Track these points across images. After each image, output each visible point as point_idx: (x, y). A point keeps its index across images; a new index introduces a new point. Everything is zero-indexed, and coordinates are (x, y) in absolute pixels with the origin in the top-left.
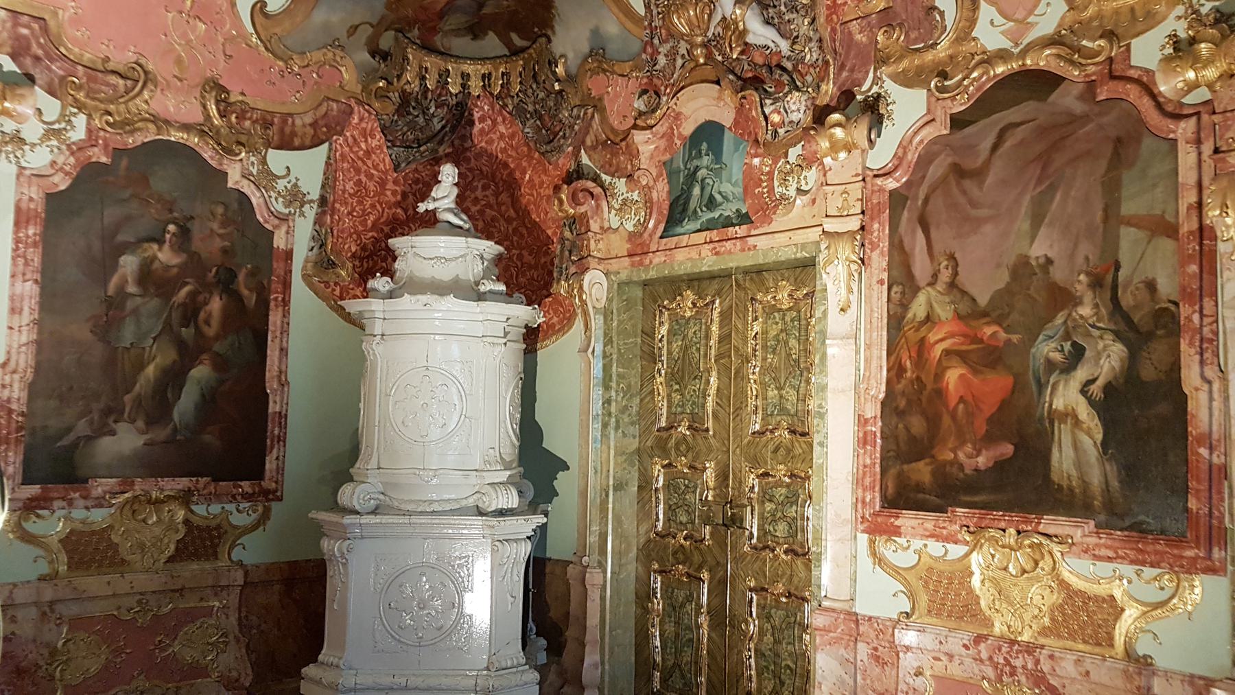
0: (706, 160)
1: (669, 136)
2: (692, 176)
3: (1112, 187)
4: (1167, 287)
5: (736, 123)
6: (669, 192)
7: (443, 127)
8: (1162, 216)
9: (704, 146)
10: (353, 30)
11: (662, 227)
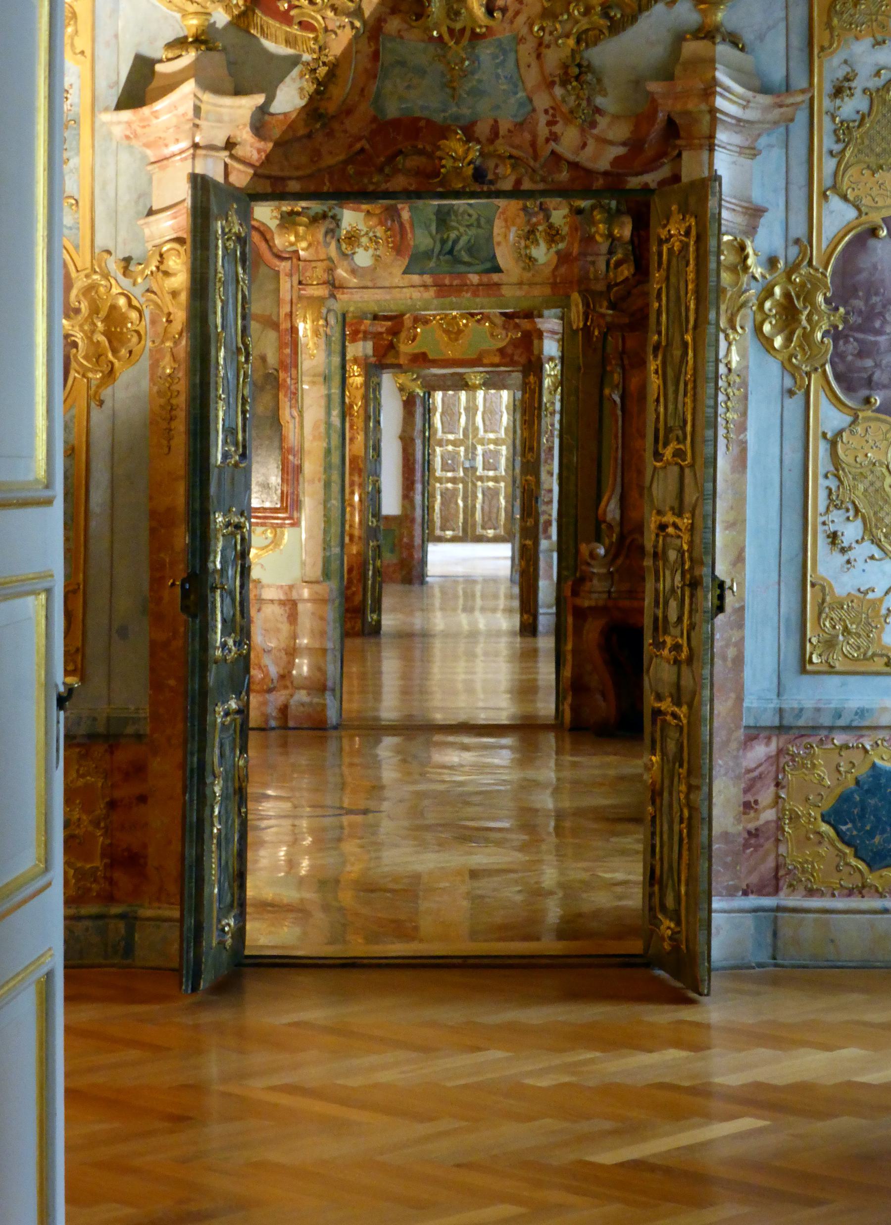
4: (272, 360)
8: (270, 316)
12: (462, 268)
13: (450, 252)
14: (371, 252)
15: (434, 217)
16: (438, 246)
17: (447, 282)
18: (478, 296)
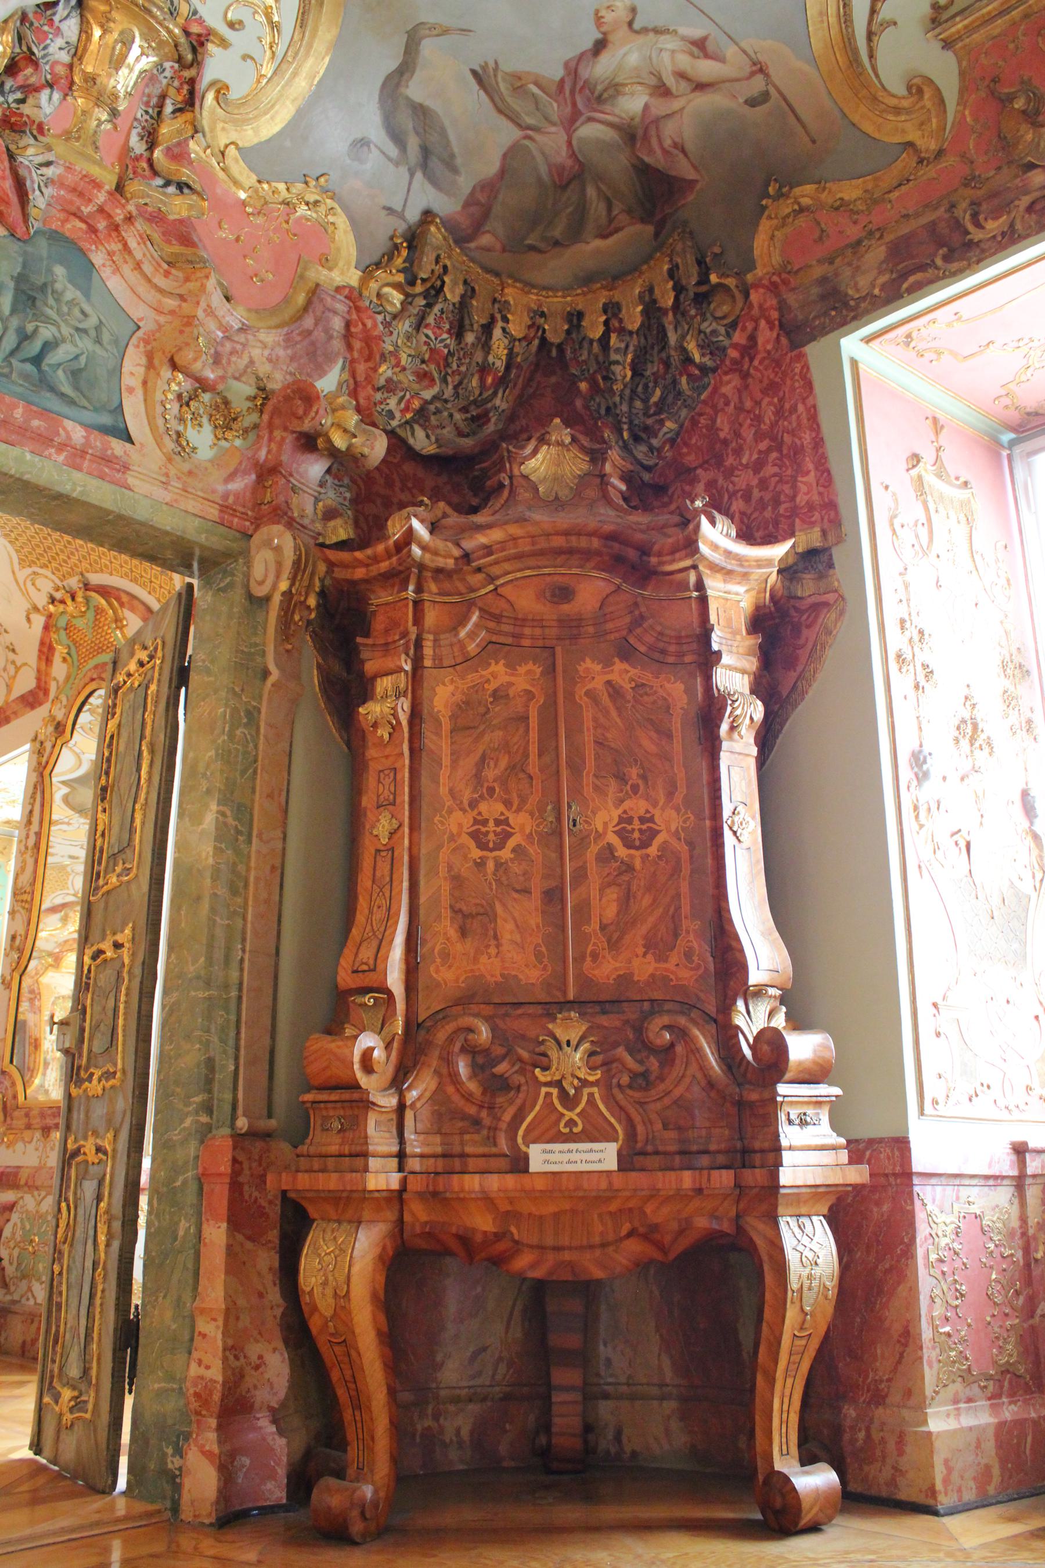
13: (37, 360)
17: (18, 413)
18: (79, 468)
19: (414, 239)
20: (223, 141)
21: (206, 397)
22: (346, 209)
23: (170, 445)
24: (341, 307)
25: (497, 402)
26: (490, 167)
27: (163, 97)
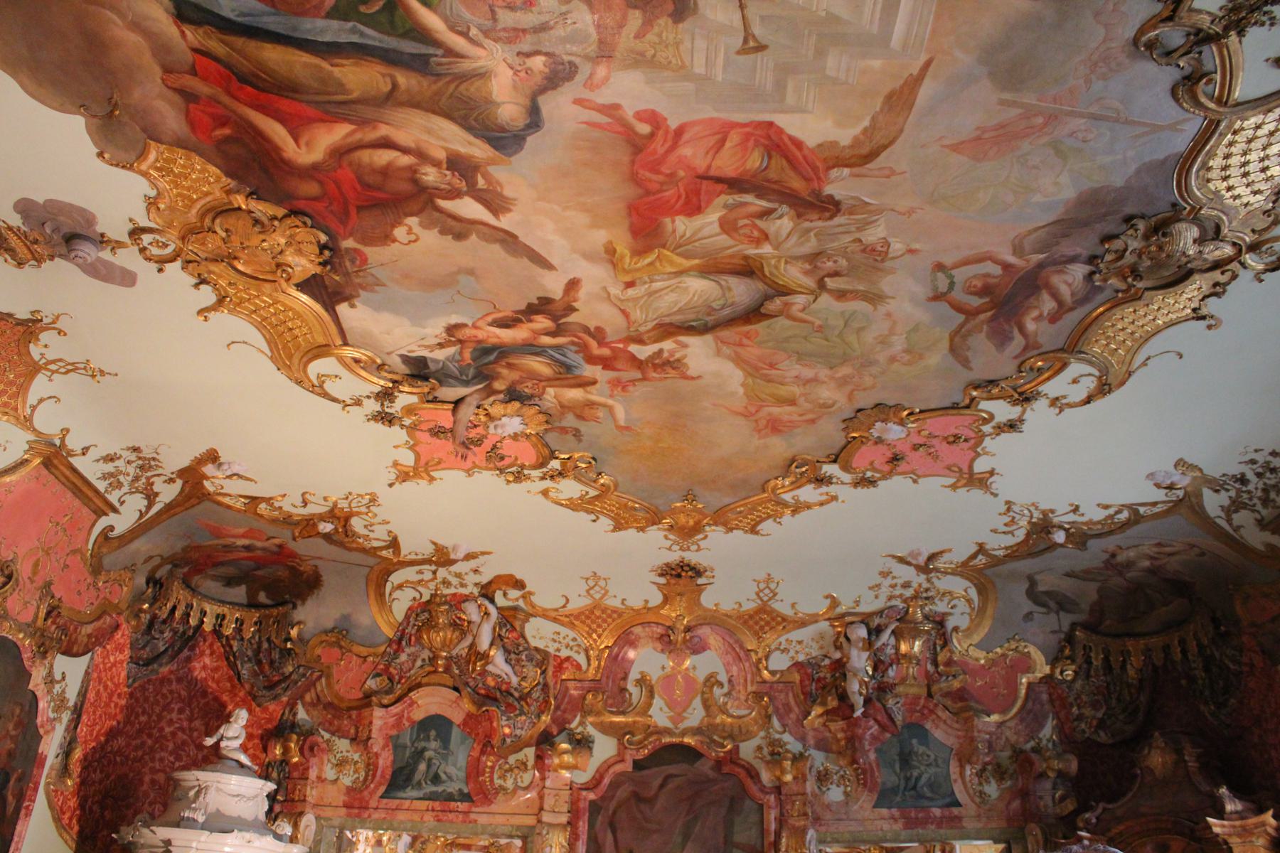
0: (433, 745)
1: (400, 717)
2: (419, 754)
3: (729, 826)
5: (465, 723)
6: (394, 762)
7: (166, 650)
9: (433, 733)
10: (151, 557)
11: (383, 789)
12: (926, 803)
14: (842, 788)
15: (897, 758)
16: (903, 782)
17: (913, 815)
19: (1070, 639)
20: (965, 646)
21: (989, 767)
22: (1034, 644)
23: (978, 800)
24: (1044, 688)
25: (1142, 698)
26: (1095, 597)
27: (935, 644)
